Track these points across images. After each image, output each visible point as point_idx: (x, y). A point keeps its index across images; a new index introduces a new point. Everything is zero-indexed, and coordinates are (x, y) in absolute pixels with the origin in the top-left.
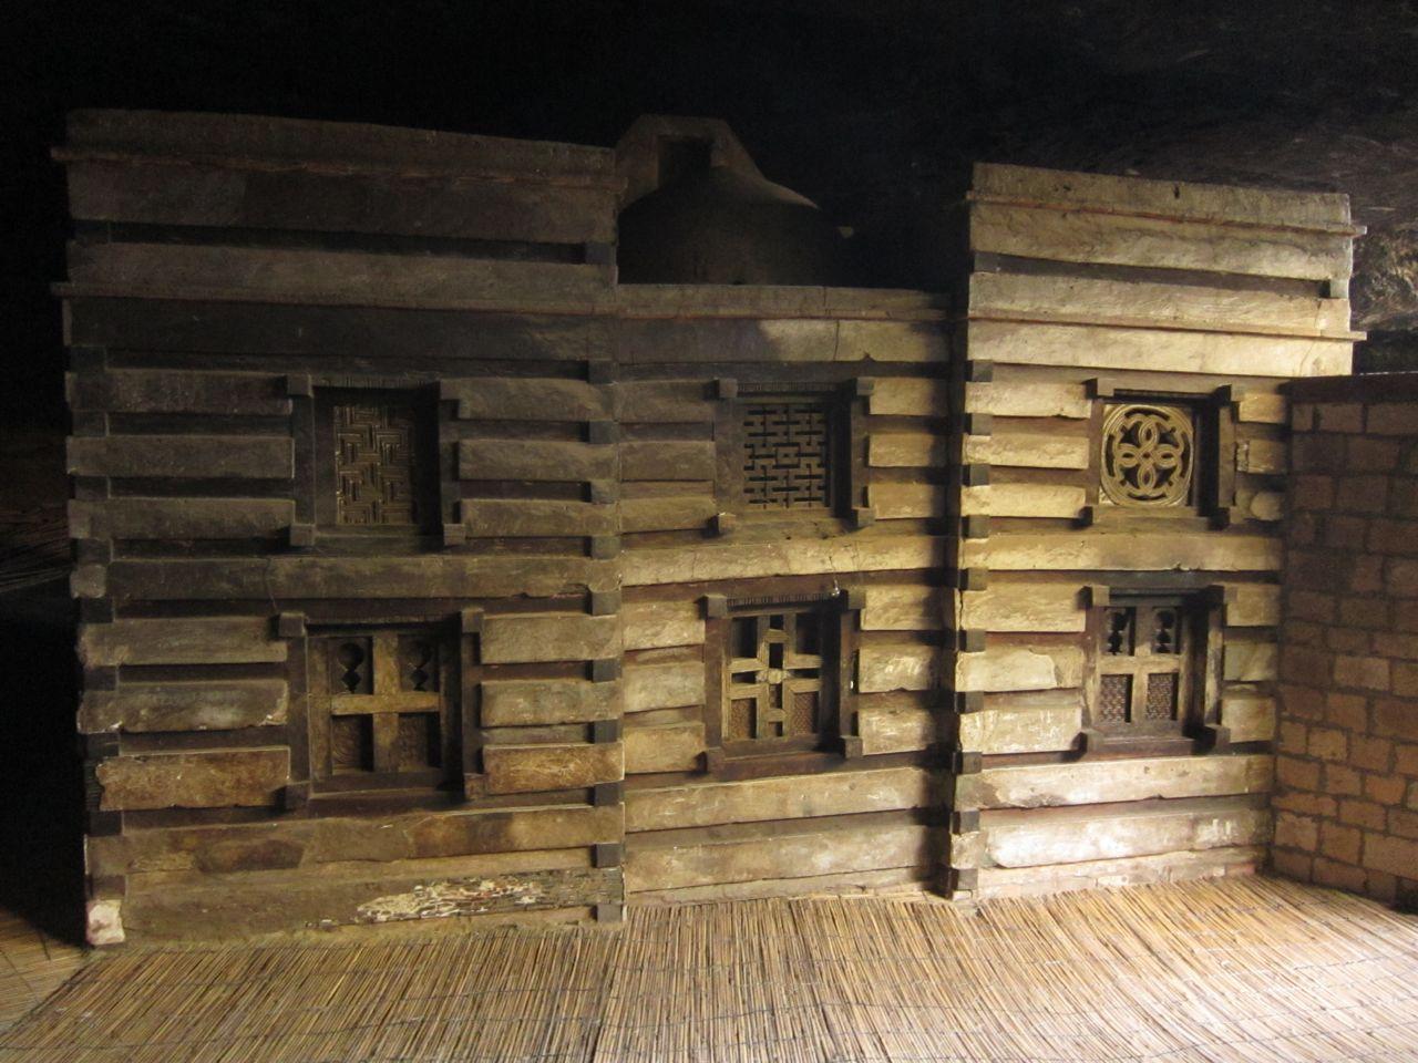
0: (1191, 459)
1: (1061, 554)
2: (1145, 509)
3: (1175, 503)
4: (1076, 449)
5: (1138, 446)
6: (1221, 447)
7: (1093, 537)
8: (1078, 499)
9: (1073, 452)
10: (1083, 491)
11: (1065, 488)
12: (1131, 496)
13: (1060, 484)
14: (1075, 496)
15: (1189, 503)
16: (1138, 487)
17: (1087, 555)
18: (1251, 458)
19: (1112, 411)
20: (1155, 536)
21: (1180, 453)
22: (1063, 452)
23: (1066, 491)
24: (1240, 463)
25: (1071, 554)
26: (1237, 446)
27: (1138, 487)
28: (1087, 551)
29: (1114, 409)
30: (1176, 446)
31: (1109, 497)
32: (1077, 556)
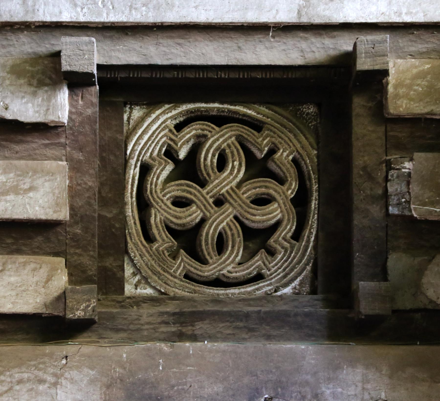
0: (314, 204)
1: (20, 382)
2: (216, 301)
3: (288, 290)
4: (39, 182)
5: (203, 184)
6: (356, 172)
7: (87, 349)
8: (49, 279)
9: (31, 189)
10: (61, 261)
11: (21, 259)
12: (187, 277)
13: (19, 252)
14: (43, 272)
15: (313, 292)
16: (204, 262)
17: (72, 381)
18: (415, 188)
19: (142, 119)
20: (222, 345)
21: (291, 194)
22: (15, 190)
23: (25, 264)
24: (394, 200)
25: (41, 381)
26: (389, 165)
27: (203, 261)
28: (74, 374)
29: (147, 115)
30: (281, 181)
31: (146, 280)
32: (55, 384)
